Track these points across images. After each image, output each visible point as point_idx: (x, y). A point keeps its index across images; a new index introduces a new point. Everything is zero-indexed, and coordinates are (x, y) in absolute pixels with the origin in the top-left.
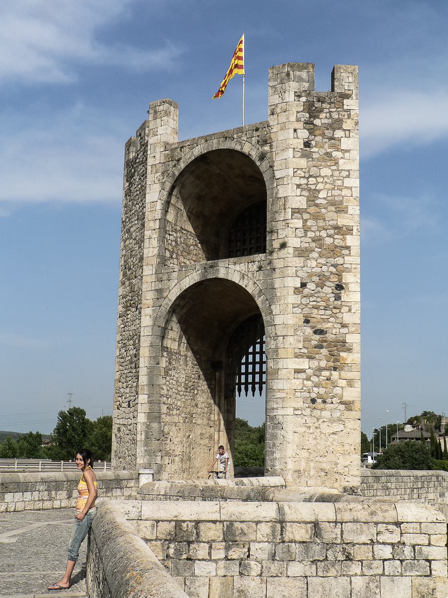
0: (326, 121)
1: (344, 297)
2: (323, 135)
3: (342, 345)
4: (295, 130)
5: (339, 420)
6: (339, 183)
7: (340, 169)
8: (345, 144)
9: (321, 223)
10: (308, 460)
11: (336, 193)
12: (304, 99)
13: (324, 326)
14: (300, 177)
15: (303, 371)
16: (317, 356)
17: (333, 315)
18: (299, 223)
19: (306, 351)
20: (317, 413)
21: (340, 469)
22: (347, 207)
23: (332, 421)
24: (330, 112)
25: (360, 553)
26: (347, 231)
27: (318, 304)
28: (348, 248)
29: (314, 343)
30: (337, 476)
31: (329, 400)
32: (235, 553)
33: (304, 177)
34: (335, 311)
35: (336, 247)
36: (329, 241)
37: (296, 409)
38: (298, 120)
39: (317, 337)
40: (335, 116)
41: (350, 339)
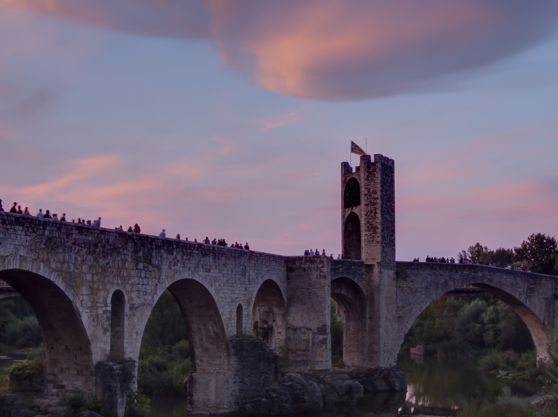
0: (371, 170)
2: (371, 174)
3: (376, 228)
4: (365, 173)
5: (376, 246)
6: (375, 186)
8: (377, 176)
10: (369, 256)
11: (374, 189)
12: (367, 165)
16: (371, 231)
17: (374, 220)
18: (366, 198)
19: (367, 230)
20: (370, 244)
21: (376, 258)
22: (377, 193)
23: (374, 246)
28: (377, 203)
29: (370, 227)
30: (376, 260)
32: (300, 262)
34: (375, 219)
35: (375, 203)
36: (373, 201)
38: (365, 170)
39: (370, 226)
40: (374, 168)
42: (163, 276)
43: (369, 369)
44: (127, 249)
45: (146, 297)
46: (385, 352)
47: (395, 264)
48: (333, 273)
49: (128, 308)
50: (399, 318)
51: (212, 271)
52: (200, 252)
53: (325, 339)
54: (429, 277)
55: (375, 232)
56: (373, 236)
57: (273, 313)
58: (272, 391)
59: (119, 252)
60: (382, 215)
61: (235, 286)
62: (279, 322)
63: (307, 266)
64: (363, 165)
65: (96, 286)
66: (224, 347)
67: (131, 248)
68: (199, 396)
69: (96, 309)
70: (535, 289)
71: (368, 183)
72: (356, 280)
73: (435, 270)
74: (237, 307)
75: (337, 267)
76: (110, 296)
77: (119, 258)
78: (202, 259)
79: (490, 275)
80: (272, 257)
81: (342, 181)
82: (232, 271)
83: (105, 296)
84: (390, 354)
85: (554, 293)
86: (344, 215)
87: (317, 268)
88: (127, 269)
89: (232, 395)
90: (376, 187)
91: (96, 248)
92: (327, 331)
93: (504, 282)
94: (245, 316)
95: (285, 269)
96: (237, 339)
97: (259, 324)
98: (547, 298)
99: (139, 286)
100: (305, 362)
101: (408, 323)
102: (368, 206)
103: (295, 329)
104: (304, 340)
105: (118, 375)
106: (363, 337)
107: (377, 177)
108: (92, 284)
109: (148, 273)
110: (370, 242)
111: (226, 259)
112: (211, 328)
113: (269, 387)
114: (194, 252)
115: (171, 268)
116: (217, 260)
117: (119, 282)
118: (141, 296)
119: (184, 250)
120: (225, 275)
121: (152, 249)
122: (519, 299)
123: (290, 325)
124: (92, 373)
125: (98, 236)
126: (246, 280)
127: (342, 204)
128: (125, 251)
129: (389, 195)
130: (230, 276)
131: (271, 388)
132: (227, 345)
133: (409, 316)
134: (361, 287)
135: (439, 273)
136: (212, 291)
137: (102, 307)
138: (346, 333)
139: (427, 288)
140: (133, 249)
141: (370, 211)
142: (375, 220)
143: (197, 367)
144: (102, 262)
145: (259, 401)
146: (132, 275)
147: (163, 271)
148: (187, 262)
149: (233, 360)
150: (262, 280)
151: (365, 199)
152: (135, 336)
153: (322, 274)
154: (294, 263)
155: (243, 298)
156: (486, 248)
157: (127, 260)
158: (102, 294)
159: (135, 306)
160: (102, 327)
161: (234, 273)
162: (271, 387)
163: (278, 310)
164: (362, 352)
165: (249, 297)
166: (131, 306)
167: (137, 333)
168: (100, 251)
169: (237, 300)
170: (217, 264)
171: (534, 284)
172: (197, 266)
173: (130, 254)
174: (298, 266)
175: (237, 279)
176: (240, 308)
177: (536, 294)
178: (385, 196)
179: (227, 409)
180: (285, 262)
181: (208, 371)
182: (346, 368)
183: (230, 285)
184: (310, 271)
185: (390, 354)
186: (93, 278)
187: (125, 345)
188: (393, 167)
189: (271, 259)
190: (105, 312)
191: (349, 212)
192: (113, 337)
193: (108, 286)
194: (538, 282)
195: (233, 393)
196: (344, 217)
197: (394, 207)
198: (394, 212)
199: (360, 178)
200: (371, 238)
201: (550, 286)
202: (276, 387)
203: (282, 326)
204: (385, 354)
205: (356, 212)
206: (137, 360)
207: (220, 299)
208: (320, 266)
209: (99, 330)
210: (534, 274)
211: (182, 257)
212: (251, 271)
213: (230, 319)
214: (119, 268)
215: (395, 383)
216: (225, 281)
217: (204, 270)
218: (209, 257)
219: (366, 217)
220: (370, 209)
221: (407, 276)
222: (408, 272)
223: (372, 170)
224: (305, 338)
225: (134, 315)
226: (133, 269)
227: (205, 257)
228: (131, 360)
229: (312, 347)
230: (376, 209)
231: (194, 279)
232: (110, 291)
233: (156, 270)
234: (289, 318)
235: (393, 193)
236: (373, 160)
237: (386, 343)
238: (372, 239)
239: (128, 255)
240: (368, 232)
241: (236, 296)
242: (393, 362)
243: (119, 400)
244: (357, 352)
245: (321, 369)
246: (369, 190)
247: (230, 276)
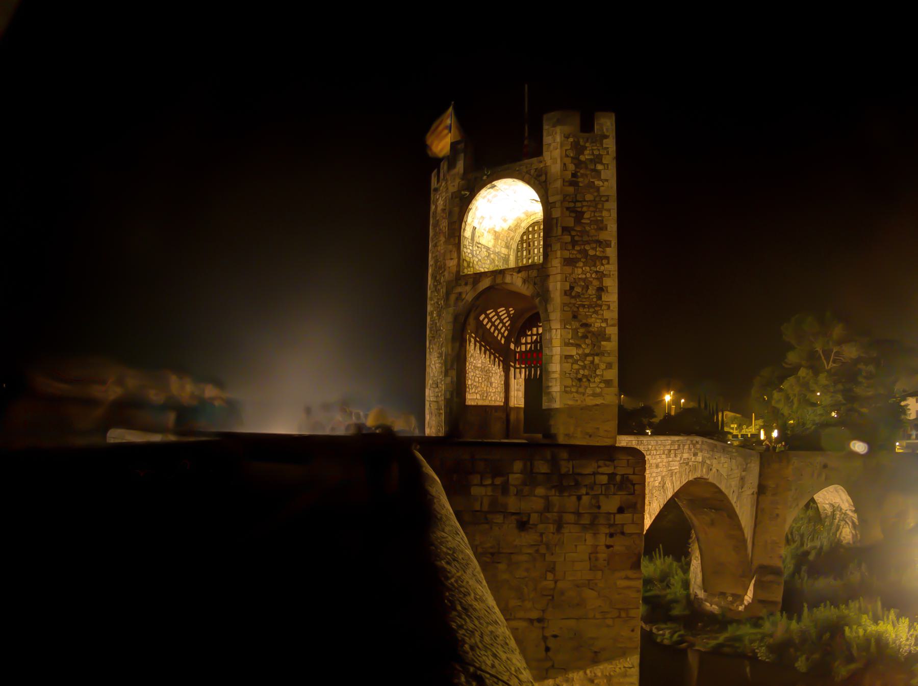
0: (587, 157)
2: (586, 168)
3: (601, 336)
4: (565, 164)
7: (601, 194)
12: (571, 140)
13: (590, 321)
14: (569, 202)
15: (572, 356)
17: (596, 312)
18: (568, 238)
20: (581, 390)
22: (607, 225)
23: (594, 395)
24: (592, 150)
27: (584, 303)
29: (580, 334)
31: (592, 380)
32: (498, 481)
33: (572, 202)
34: (597, 309)
36: (591, 253)
37: (565, 387)
56: (592, 362)
63: (538, 504)
87: (595, 517)
107: (607, 180)
110: (580, 380)
142: (601, 312)
151: (566, 243)
174: (486, 502)
184: (552, 528)
200: (584, 367)
208: (611, 504)
219: (567, 299)
220: (584, 276)
223: (592, 157)
230: (601, 276)
240: (575, 348)
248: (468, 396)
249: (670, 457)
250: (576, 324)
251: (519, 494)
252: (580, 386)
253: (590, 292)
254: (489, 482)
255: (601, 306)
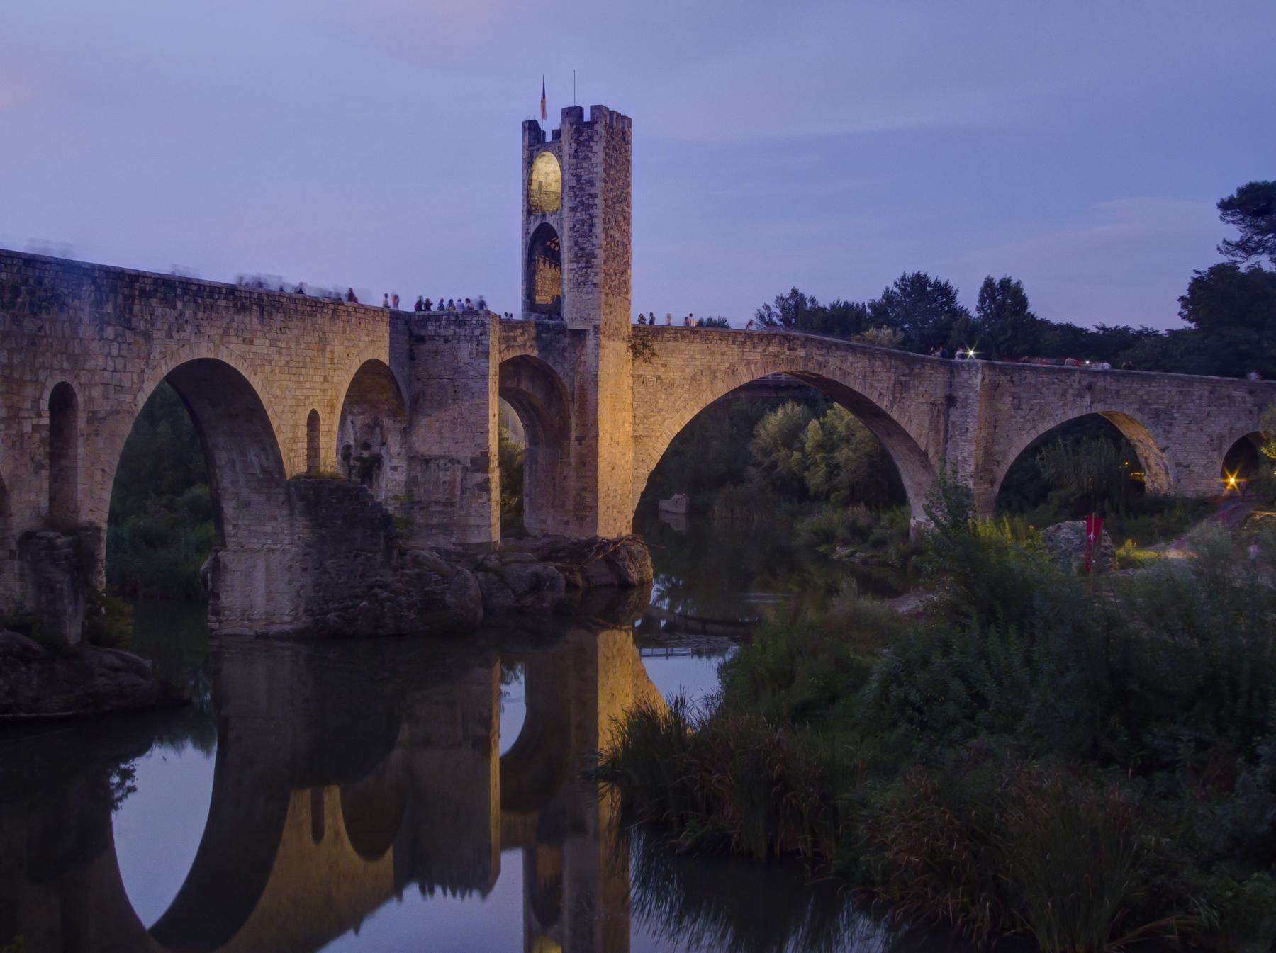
0: (585, 138)
1: (594, 230)
2: (584, 146)
3: (593, 255)
4: (570, 144)
8: (594, 149)
9: (583, 193)
10: (576, 313)
11: (590, 176)
12: (574, 127)
15: (574, 269)
16: (581, 262)
17: (588, 240)
18: (572, 194)
19: (575, 259)
23: (587, 293)
25: (468, 323)
26: (594, 196)
28: (596, 205)
29: (579, 255)
32: (438, 323)
36: (586, 202)
37: (571, 288)
38: (572, 138)
39: (581, 252)
41: (596, 252)
42: (156, 354)
43: (576, 541)
44: (80, 298)
45: (121, 397)
46: (608, 508)
47: (630, 330)
48: (503, 346)
49: (85, 420)
50: (636, 437)
51: (256, 342)
52: (231, 305)
53: (487, 481)
54: (699, 356)
55: (590, 265)
56: (586, 272)
57: (381, 427)
58: (380, 587)
59: (63, 304)
60: (606, 231)
61: (303, 373)
62: (394, 445)
63: (451, 332)
64: (568, 126)
65: (16, 375)
66: (282, 498)
67: (90, 295)
68: (231, 598)
69: (20, 423)
70: (911, 386)
71: (577, 164)
72: (550, 363)
73: (711, 343)
74: (307, 416)
75: (511, 334)
76: (47, 395)
77: (64, 317)
78: (236, 318)
79: (821, 355)
80: (380, 314)
81: (524, 159)
82: (298, 342)
83: (37, 396)
84: (618, 512)
85: (948, 393)
86: (528, 229)
87: (471, 337)
88: (81, 340)
89: (300, 596)
90: (592, 173)
91: (17, 296)
92: (492, 466)
93: (849, 371)
94: (324, 433)
95: (406, 337)
96: (308, 480)
97: (352, 451)
98: (933, 403)
99: (105, 372)
100: (446, 528)
101: (654, 449)
102: (576, 212)
103: (427, 461)
104: (444, 482)
105: (66, 558)
106: (565, 477)
107: (596, 153)
108: (8, 371)
109: (125, 346)
110: (579, 284)
111: (285, 316)
112: (255, 460)
113: (374, 579)
114: (218, 303)
115: (171, 337)
116: (266, 320)
117: (65, 365)
118: (112, 395)
119: (200, 300)
120: (284, 351)
121: (132, 297)
122: (878, 404)
123: (417, 452)
124: (12, 552)
125: (19, 272)
126: (327, 361)
127: (523, 206)
128: (76, 302)
129: (620, 190)
130: (293, 352)
131: (377, 581)
132: (288, 493)
133: (658, 434)
134: (561, 375)
135: (719, 349)
136: (256, 382)
137: (31, 418)
138: (531, 467)
139: (693, 379)
140: (92, 297)
141: (580, 222)
143: (228, 539)
144: (29, 325)
145: (355, 606)
146: (91, 352)
147: (155, 342)
148: (205, 323)
149: (301, 523)
150: (360, 361)
152: (98, 478)
153: (480, 349)
154: (425, 327)
155: (319, 398)
156: (813, 300)
157: (80, 320)
158: (29, 391)
159: (99, 415)
160: (32, 459)
161: (302, 347)
162: (378, 578)
163: (391, 422)
164: (563, 506)
165: (332, 396)
166: (91, 414)
167: (103, 470)
168: (24, 304)
169: (307, 402)
170: (267, 328)
171: (909, 375)
172: (226, 332)
173: (87, 309)
175: (308, 360)
176: (313, 418)
177: (913, 395)
178: (612, 190)
179: (290, 623)
180: (407, 323)
181: (251, 546)
182: (530, 539)
183: (294, 370)
184: (456, 342)
185: (618, 512)
186: (10, 359)
187: (80, 496)
188: (629, 133)
189: (378, 318)
190: (36, 428)
191: (538, 223)
192: (54, 479)
193: (42, 375)
194: (917, 371)
195: (302, 592)
196: (527, 233)
197: (629, 213)
198: (629, 224)
199: (561, 154)
200: (581, 276)
201: (939, 379)
202: (390, 579)
203: (399, 454)
204: (610, 511)
205: (551, 223)
206: (105, 526)
207: (273, 400)
209: (26, 465)
210: (908, 355)
211: (195, 314)
212: (337, 343)
213: (294, 440)
214: (63, 336)
215: (629, 570)
216: (283, 363)
217: (241, 339)
218: (251, 314)
219: (571, 233)
220: (581, 217)
221: (654, 354)
222: (656, 345)
223: (587, 138)
224: (447, 478)
225: (96, 435)
226: (94, 339)
227: (243, 314)
228: (93, 528)
229: (462, 498)
230: (592, 217)
231: (220, 358)
232: (47, 384)
233: (141, 341)
234: (414, 438)
235: (628, 185)
236: (587, 117)
237: (610, 488)
238: (583, 278)
239: (82, 310)
241: (306, 393)
242: (625, 527)
243: (70, 609)
244: (553, 507)
245: (479, 541)
246: (578, 178)
247: (293, 352)
248: (537, 298)
249: (744, 347)
250: (577, 249)
251: (445, 329)
252: (579, 288)
253: (585, 227)
254: (434, 324)
255: (591, 236)
